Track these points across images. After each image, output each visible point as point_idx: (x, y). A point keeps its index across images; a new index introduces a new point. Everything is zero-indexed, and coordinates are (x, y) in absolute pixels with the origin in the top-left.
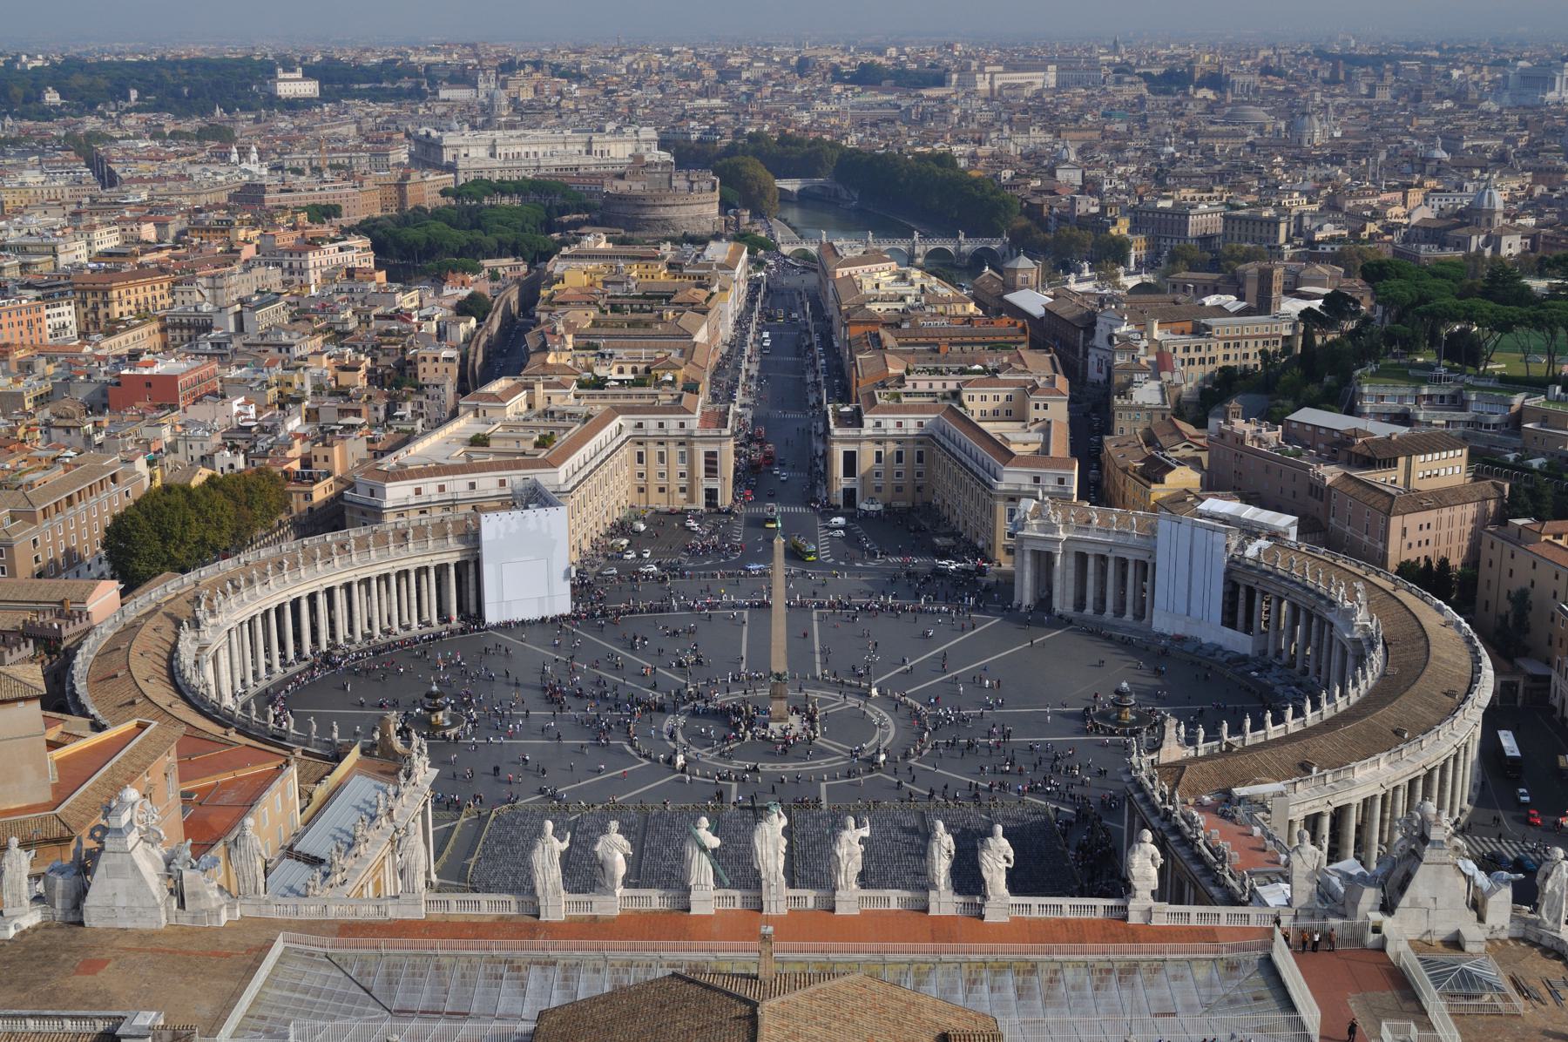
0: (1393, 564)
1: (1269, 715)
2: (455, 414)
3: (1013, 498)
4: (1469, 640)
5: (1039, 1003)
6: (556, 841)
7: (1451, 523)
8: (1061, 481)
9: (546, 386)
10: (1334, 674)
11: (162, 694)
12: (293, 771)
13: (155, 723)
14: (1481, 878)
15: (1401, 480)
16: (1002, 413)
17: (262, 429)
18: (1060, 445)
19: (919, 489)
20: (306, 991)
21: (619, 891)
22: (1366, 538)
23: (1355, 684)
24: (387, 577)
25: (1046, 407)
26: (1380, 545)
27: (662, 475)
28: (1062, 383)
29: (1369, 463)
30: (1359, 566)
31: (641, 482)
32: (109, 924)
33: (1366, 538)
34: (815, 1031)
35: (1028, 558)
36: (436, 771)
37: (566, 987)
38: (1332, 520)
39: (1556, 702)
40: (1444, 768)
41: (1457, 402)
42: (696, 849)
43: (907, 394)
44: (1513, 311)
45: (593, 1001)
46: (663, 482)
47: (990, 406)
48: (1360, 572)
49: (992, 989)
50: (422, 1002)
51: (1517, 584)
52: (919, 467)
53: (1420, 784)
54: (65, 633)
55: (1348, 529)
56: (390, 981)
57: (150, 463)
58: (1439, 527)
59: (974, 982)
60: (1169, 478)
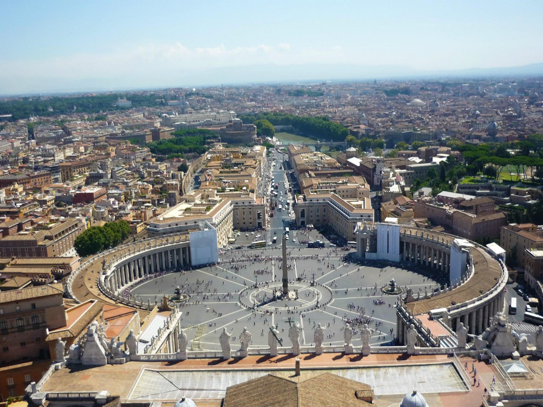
3: (355, 223)
5: (382, 380)
8: (369, 216)
11: (95, 291)
13: (96, 301)
19: (324, 220)
22: (465, 231)
23: (466, 276)
24: (161, 253)
28: (368, 186)
32: (90, 364)
33: (465, 231)
36: (181, 313)
38: (454, 226)
39: (527, 280)
41: (490, 188)
44: (506, 160)
45: (244, 384)
46: (244, 221)
49: (367, 376)
52: (324, 214)
53: (487, 307)
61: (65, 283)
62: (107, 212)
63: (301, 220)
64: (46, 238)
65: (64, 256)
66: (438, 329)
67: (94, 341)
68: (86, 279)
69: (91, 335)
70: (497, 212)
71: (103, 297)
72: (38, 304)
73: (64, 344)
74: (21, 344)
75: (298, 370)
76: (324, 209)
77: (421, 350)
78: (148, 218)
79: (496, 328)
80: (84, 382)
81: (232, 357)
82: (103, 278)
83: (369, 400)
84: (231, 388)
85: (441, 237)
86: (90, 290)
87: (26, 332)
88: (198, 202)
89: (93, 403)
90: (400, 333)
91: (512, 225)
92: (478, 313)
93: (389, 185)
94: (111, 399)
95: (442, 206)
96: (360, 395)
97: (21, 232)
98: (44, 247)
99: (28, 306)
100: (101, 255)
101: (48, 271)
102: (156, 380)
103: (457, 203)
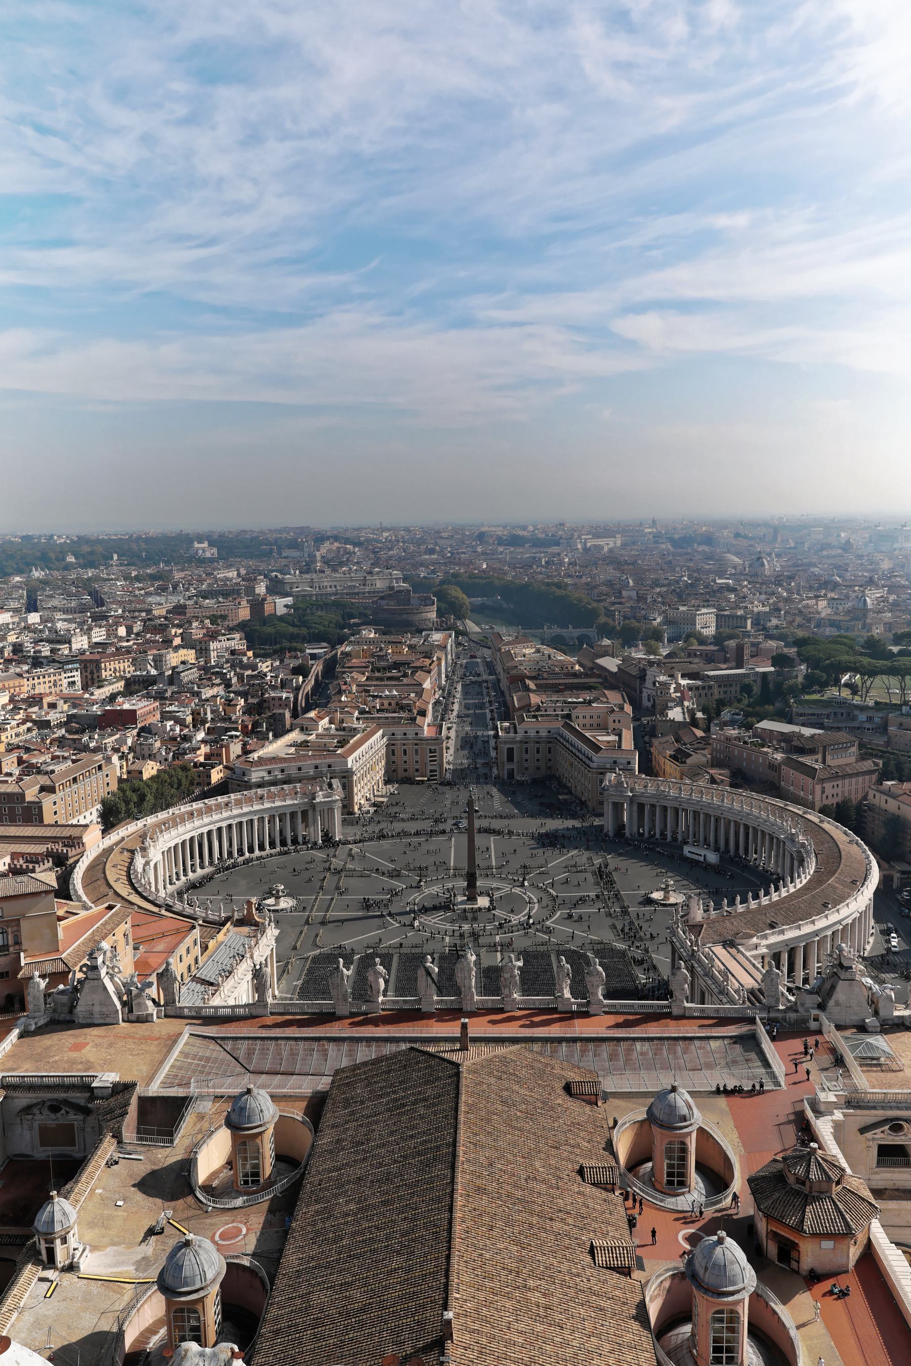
0: (818, 805)
1: (750, 894)
2: (291, 730)
3: (602, 772)
4: (864, 852)
6: (344, 970)
7: (850, 785)
8: (629, 763)
9: (341, 713)
11: (123, 889)
12: (196, 933)
14: (876, 987)
15: (820, 760)
16: (595, 725)
17: (186, 738)
18: (628, 742)
19: (549, 768)
20: (200, 1059)
21: (381, 999)
22: (802, 793)
23: (799, 876)
24: (252, 820)
25: (619, 721)
26: (811, 797)
27: (405, 762)
28: (628, 708)
29: (802, 751)
30: (799, 809)
31: (393, 767)
32: (89, 1021)
34: (493, 1080)
35: (610, 807)
36: (276, 932)
37: (351, 1055)
38: (782, 783)
40: (853, 924)
42: (424, 973)
43: (542, 716)
45: (365, 1064)
47: (588, 721)
48: (800, 813)
50: (267, 1067)
52: (549, 756)
54: (70, 855)
55: (792, 788)
56: (250, 1053)
57: (121, 758)
58: (843, 786)
59: (585, 1051)
60: (689, 761)
63: (508, 766)
65: (75, 822)
67: (99, 979)
69: (95, 968)
73: (43, 984)
76: (549, 748)
77: (695, 1009)
78: (232, 756)
79: (835, 973)
84: (343, 1070)
88: (320, 730)
89: (88, 1095)
91: (889, 783)
93: (667, 708)
94: (120, 1088)
95: (763, 746)
100: (140, 824)
101: (40, 849)
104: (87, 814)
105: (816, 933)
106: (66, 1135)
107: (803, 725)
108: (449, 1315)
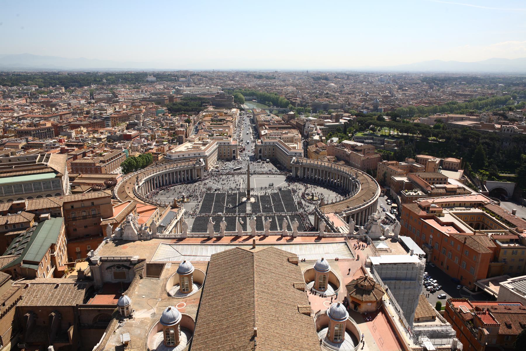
3: (291, 157)
10: (351, 190)
11: (132, 195)
17: (149, 144)
28: (300, 136)
45: (221, 253)
47: (286, 140)
51: (384, 172)
61: (112, 190)
62: (139, 147)
63: (259, 155)
64: (101, 161)
66: (338, 223)
68: (126, 188)
69: (129, 222)
70: (376, 153)
71: (136, 199)
72: (96, 202)
74: (85, 227)
75: (254, 245)
78: (165, 151)
80: (123, 250)
81: (215, 237)
82: (137, 187)
83: (296, 263)
85: (342, 168)
86: (129, 194)
87: (88, 219)
88: (196, 142)
90: (316, 224)
92: (362, 213)
93: (312, 135)
96: (290, 260)
97: (85, 158)
98: (100, 168)
99: (89, 204)
100: (136, 173)
101: (102, 182)
102: (168, 250)
103: (353, 148)
104: (116, 170)
105: (361, 210)
106: (123, 275)
107: (357, 142)
108: (256, 329)
